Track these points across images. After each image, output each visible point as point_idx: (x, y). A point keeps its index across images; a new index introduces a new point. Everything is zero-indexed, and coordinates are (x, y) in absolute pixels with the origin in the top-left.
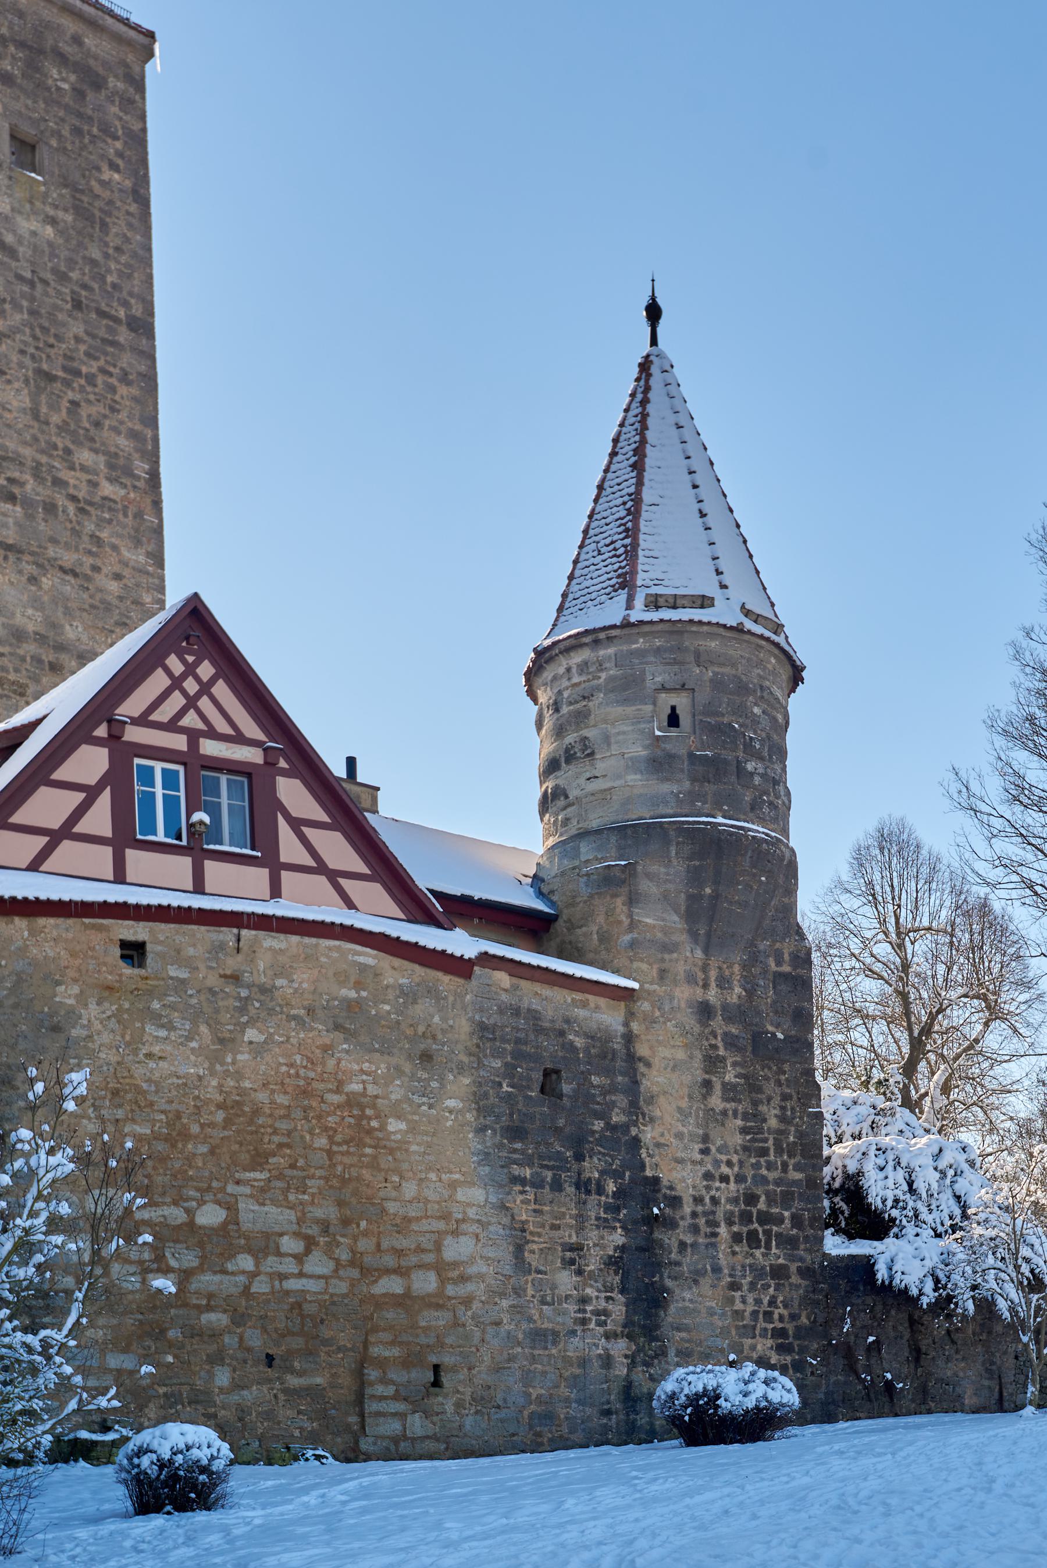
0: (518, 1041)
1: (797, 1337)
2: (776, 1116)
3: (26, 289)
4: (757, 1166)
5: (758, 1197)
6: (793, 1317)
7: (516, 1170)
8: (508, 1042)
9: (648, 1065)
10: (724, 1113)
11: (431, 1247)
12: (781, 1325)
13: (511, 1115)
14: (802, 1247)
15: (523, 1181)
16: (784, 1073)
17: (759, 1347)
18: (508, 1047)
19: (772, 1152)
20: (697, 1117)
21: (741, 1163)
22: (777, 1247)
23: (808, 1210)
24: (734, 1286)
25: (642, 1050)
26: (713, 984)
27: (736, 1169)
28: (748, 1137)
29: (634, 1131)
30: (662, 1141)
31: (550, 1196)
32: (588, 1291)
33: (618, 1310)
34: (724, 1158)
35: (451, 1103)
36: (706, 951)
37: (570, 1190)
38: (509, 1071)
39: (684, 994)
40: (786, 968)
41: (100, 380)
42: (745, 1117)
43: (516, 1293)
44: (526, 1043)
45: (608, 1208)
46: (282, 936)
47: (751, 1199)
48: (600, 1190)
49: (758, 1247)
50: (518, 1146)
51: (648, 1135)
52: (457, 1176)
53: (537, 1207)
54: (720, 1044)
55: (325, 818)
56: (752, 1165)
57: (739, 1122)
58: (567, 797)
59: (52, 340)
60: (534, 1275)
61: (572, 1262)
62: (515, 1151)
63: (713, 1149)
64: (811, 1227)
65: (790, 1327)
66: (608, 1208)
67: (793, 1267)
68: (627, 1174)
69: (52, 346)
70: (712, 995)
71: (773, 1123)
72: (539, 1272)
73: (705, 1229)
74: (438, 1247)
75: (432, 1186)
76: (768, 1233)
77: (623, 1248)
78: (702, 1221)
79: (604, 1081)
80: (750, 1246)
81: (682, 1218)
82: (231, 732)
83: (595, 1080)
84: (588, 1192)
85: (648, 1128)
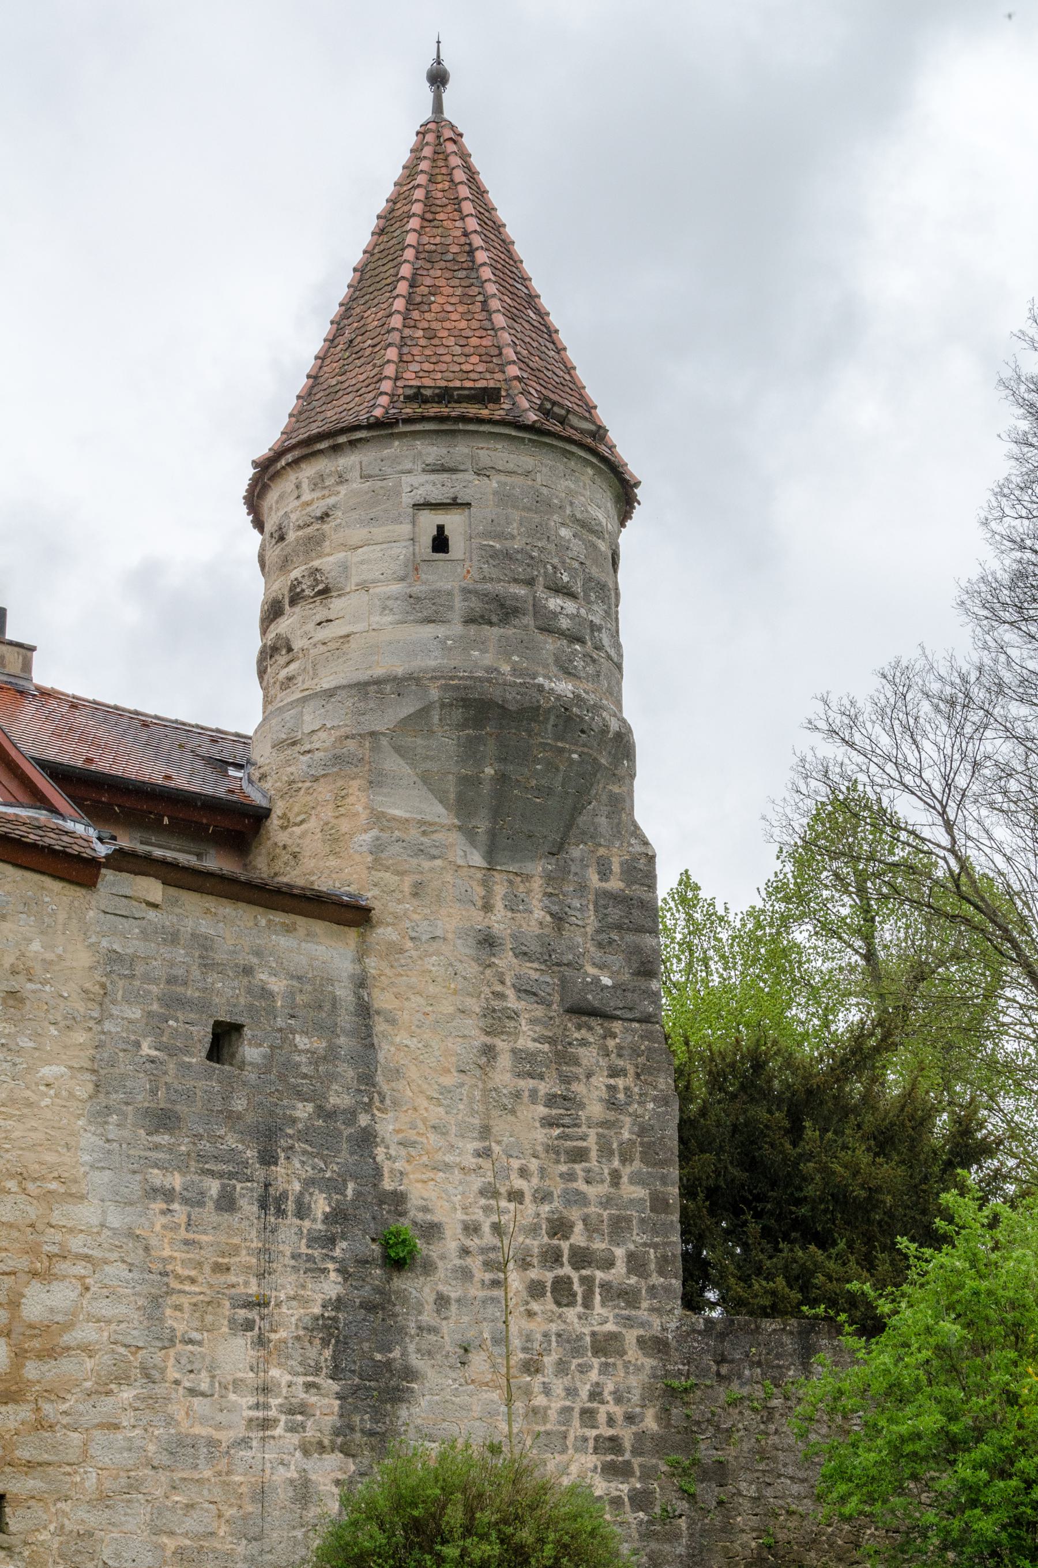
0: (172, 980)
1: (636, 1452)
2: (601, 1100)
4: (571, 1177)
6: (630, 1418)
7: (156, 1176)
8: (155, 981)
9: (392, 1021)
10: (517, 1095)
12: (610, 1432)
13: (154, 1092)
14: (645, 1304)
15: (168, 1195)
16: (614, 1036)
17: (574, 1469)
18: (154, 988)
19: (594, 1154)
20: (471, 1100)
22: (603, 1304)
23: (655, 1246)
24: (532, 1367)
25: (382, 1000)
26: (499, 905)
27: (535, 1181)
28: (557, 1132)
29: (363, 1120)
30: (412, 1135)
31: (215, 1218)
32: (275, 1372)
33: (326, 1406)
34: (516, 1164)
35: (47, 1071)
36: (491, 854)
37: (249, 1207)
38: (155, 1024)
39: (453, 919)
40: (615, 884)
42: (551, 1100)
43: (148, 1376)
45: (314, 1240)
47: (560, 1227)
48: (302, 1211)
49: (572, 1304)
50: (164, 1139)
51: (388, 1126)
52: (53, 1186)
53: (190, 1236)
54: (510, 993)
56: (561, 1175)
57: (542, 1110)
60: (179, 1347)
62: (157, 1147)
63: (496, 1148)
64: (661, 1273)
65: (627, 1435)
66: (314, 1240)
67: (631, 1336)
68: (351, 1186)
70: (499, 921)
71: (595, 1110)
72: (191, 1341)
73: (480, 1274)
76: (587, 1282)
77: (339, 1304)
78: (475, 1263)
80: (559, 1304)
81: (443, 1257)
83: (301, 1041)
84: (281, 1213)
85: (391, 1114)
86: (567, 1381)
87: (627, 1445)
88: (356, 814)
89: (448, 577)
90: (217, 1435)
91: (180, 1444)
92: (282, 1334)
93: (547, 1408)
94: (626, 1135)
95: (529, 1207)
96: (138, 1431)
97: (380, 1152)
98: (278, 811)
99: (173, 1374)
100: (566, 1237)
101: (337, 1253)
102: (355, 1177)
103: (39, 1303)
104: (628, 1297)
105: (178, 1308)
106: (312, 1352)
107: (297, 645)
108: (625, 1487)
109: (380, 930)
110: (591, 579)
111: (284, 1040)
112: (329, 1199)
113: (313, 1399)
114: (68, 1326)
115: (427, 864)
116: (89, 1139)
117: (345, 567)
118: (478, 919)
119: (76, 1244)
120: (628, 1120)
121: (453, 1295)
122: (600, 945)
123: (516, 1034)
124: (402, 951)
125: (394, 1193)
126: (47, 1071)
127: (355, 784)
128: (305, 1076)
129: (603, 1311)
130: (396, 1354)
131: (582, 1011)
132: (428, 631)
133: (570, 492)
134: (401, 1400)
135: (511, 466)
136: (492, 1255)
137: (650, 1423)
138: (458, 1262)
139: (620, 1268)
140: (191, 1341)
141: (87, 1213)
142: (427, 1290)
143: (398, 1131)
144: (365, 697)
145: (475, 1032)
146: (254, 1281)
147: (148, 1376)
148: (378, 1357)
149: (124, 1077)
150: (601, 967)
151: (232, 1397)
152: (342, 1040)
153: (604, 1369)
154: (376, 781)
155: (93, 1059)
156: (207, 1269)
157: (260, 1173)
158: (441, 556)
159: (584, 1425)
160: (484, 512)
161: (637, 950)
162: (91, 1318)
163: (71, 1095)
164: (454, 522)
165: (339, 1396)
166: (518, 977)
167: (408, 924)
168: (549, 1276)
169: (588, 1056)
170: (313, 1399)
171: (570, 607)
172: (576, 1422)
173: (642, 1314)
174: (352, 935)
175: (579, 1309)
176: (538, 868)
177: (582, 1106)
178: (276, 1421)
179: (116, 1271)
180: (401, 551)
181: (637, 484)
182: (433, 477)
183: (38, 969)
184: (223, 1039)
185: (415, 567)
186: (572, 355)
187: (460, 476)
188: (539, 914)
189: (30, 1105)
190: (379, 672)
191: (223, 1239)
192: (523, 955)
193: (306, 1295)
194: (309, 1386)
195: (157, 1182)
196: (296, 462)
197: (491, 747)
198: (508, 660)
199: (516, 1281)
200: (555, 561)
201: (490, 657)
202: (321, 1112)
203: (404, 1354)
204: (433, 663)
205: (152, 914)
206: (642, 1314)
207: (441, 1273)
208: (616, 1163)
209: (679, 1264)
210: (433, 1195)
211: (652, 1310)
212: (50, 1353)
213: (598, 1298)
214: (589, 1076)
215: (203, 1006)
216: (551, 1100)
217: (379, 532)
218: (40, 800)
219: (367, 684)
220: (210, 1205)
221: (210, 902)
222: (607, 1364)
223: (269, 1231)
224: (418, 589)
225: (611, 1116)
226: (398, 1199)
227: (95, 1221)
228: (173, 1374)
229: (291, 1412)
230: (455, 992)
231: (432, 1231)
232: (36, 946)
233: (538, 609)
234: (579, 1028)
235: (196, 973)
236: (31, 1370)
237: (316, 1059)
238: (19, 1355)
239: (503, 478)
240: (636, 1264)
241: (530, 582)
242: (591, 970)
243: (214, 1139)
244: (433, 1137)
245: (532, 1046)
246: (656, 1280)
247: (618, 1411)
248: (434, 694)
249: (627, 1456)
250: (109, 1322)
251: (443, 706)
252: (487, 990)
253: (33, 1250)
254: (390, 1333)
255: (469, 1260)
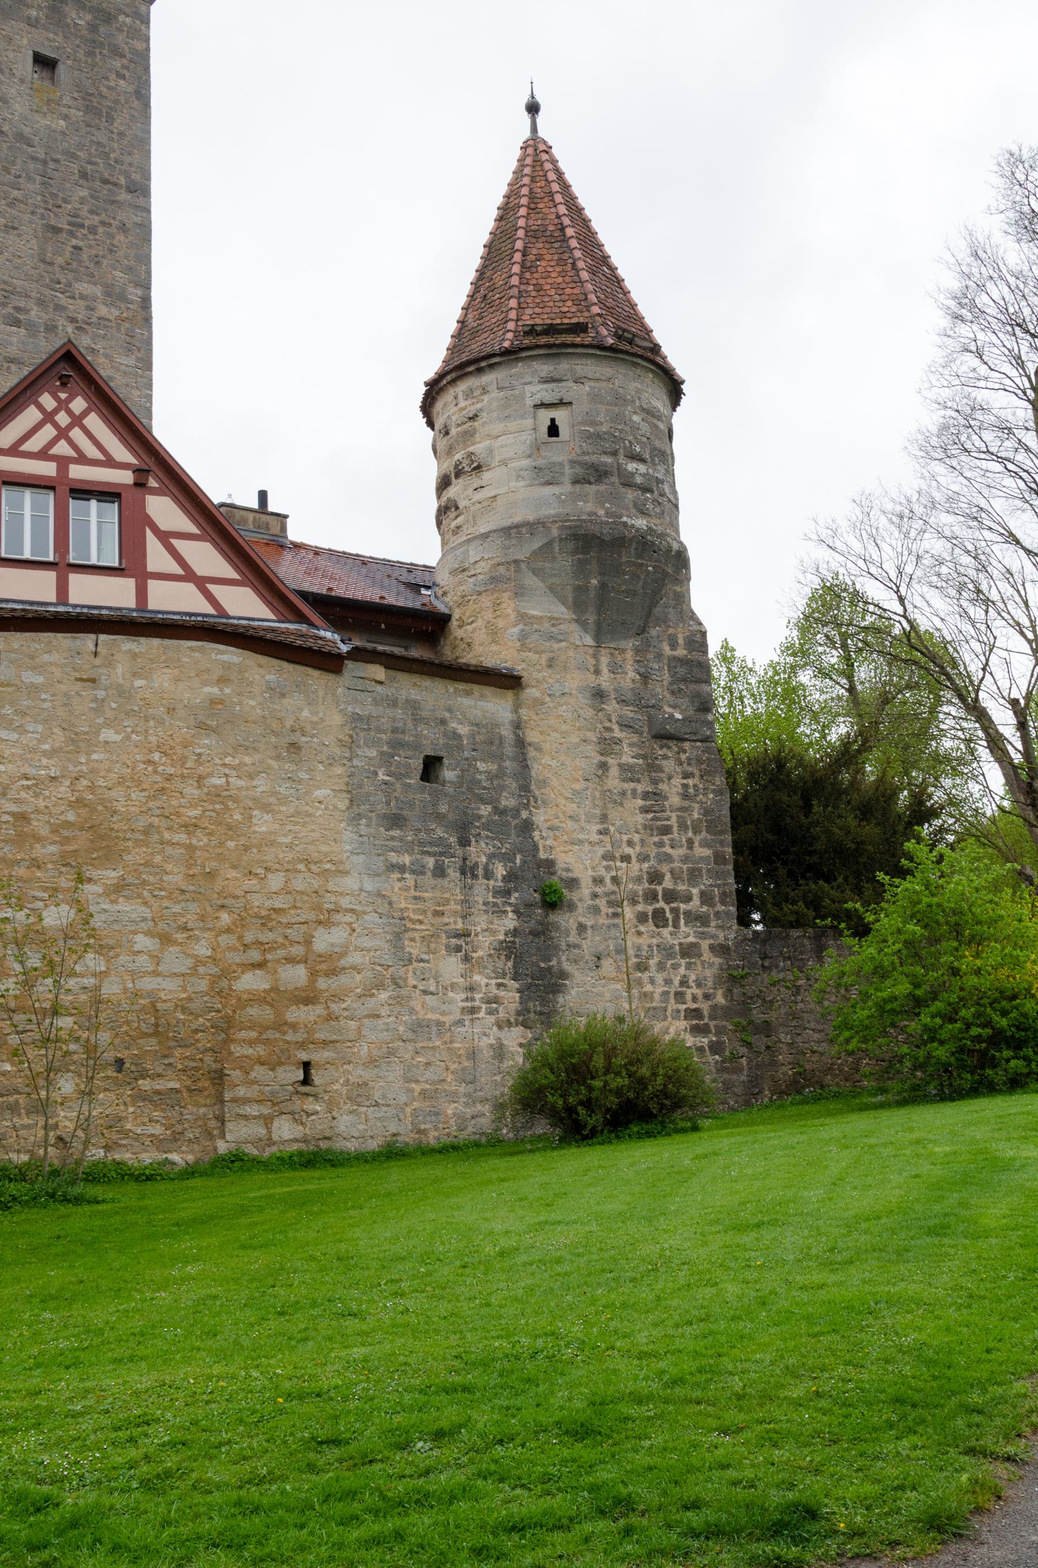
0: (395, 730)
1: (711, 1018)
2: (678, 794)
3: (39, 166)
4: (660, 844)
5: (663, 876)
6: (707, 997)
7: (393, 857)
8: (384, 732)
9: (539, 749)
10: (623, 793)
11: (300, 939)
12: (695, 1006)
13: (388, 803)
14: (713, 924)
15: (402, 868)
16: (685, 752)
17: (672, 1030)
18: (384, 736)
19: (675, 829)
20: (594, 798)
21: (642, 841)
22: (686, 924)
23: (718, 886)
24: (642, 967)
25: (532, 736)
26: (605, 670)
27: (638, 848)
28: (650, 816)
29: (524, 814)
30: (556, 823)
31: (432, 882)
32: (477, 978)
33: (511, 997)
34: (625, 838)
35: (319, 793)
36: (598, 637)
37: (454, 874)
38: (386, 759)
39: (576, 681)
40: (681, 652)
41: (101, 230)
42: (646, 796)
43: (396, 984)
44: (403, 732)
45: (497, 893)
46: (142, 640)
47: (655, 877)
48: (488, 875)
49: (666, 926)
50: (396, 833)
51: (540, 817)
52: (328, 866)
53: (418, 894)
54: (616, 727)
55: (194, 530)
57: (640, 802)
58: (457, 508)
59: (60, 202)
60: (415, 964)
61: (458, 949)
62: (392, 838)
63: (612, 829)
64: (723, 903)
65: (705, 1007)
66: (497, 893)
67: (705, 944)
68: (519, 857)
69: (59, 207)
70: (605, 680)
71: (675, 800)
72: (422, 961)
73: (605, 909)
74: (308, 942)
75: (301, 876)
76: (675, 911)
77: (515, 932)
78: (602, 903)
79: (493, 767)
80: (657, 926)
81: (581, 900)
82: (102, 457)
83: (481, 766)
86: (665, 974)
87: (706, 1013)
88: (508, 615)
89: (560, 453)
90: (442, 1019)
91: (420, 1025)
92: (480, 953)
93: (653, 993)
94: (696, 816)
95: (635, 866)
96: (392, 1019)
97: (536, 833)
98: (456, 616)
99: (412, 982)
100: (660, 883)
101: (513, 900)
102: (521, 852)
103: (324, 940)
104: (702, 920)
105: (413, 940)
106: (500, 964)
107: (462, 504)
108: (706, 1040)
109: (528, 691)
110: (655, 449)
111: (470, 765)
112: (505, 866)
113: (503, 994)
114: (343, 955)
115: (556, 646)
116: (348, 835)
117: (490, 451)
118: (591, 680)
119: (345, 902)
120: (697, 805)
121: (589, 924)
122: (673, 693)
123: (620, 754)
124: (543, 704)
125: (547, 860)
126: (319, 793)
127: (506, 595)
128: (485, 788)
129: (687, 930)
130: (554, 963)
131: (663, 737)
132: (549, 490)
133: (638, 391)
134: (559, 991)
135: (597, 375)
136: (613, 897)
137: (720, 999)
138: (591, 902)
139: (696, 901)
140: (422, 961)
141: (350, 883)
142: (571, 921)
143: (547, 821)
144: (509, 537)
145: (594, 754)
146: (460, 920)
147: (396, 984)
148: (543, 965)
149: (368, 794)
150: (674, 707)
151: (451, 994)
152: (508, 763)
153: (689, 966)
154: (519, 593)
155: (347, 784)
156: (429, 915)
157: (459, 852)
158: (554, 439)
159: (677, 1002)
160: (582, 407)
161: (698, 695)
162: (357, 948)
163: (335, 808)
164: (561, 416)
165: (519, 991)
166: (620, 717)
167: (546, 686)
168: (650, 909)
169: (669, 766)
170: (503, 994)
171: (642, 468)
172: (672, 1000)
173: (712, 930)
174: (510, 694)
175: (671, 929)
176: (629, 644)
177: (666, 798)
178: (480, 1008)
179: (371, 918)
180: (527, 437)
181: (683, 382)
182: (546, 386)
183: (308, 728)
184: (431, 767)
185: (537, 448)
186: (635, 296)
187: (564, 384)
188: (631, 674)
189: (310, 815)
190: (517, 519)
191: (438, 894)
192: (623, 702)
193: (493, 928)
194: (499, 985)
195: (394, 861)
196: (453, 381)
197: (594, 566)
198: (603, 507)
199: (629, 912)
200: (631, 438)
201: (590, 506)
202: (496, 810)
203: (559, 962)
204: (553, 512)
205: (379, 688)
206: (712, 930)
207: (580, 910)
208: (690, 834)
209: (734, 897)
210: (572, 861)
211: (718, 927)
212: (333, 972)
213: (682, 921)
214: (669, 779)
215: (416, 746)
216: (646, 796)
217: (512, 425)
218: (302, 618)
219: (510, 528)
220: (429, 873)
221: (416, 679)
222: (690, 963)
223: (467, 888)
224: (540, 462)
225: (686, 804)
226: (550, 864)
227: (356, 887)
228: (412, 982)
229: (489, 1002)
230: (579, 729)
231: (573, 883)
232: (306, 713)
233: (620, 470)
234: (661, 747)
235: (410, 724)
236: (322, 983)
237: (491, 777)
238: (313, 974)
239: (592, 384)
240: (706, 898)
241: (614, 454)
242: (668, 709)
243: (429, 831)
244: (570, 823)
245: (632, 761)
246: (720, 908)
247: (699, 992)
248: (555, 532)
249: (706, 1021)
250: (369, 951)
251: (561, 540)
252: (600, 726)
253: (318, 908)
254: (549, 950)
255: (597, 901)
